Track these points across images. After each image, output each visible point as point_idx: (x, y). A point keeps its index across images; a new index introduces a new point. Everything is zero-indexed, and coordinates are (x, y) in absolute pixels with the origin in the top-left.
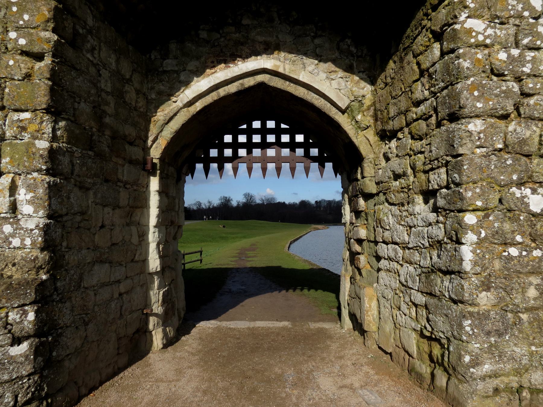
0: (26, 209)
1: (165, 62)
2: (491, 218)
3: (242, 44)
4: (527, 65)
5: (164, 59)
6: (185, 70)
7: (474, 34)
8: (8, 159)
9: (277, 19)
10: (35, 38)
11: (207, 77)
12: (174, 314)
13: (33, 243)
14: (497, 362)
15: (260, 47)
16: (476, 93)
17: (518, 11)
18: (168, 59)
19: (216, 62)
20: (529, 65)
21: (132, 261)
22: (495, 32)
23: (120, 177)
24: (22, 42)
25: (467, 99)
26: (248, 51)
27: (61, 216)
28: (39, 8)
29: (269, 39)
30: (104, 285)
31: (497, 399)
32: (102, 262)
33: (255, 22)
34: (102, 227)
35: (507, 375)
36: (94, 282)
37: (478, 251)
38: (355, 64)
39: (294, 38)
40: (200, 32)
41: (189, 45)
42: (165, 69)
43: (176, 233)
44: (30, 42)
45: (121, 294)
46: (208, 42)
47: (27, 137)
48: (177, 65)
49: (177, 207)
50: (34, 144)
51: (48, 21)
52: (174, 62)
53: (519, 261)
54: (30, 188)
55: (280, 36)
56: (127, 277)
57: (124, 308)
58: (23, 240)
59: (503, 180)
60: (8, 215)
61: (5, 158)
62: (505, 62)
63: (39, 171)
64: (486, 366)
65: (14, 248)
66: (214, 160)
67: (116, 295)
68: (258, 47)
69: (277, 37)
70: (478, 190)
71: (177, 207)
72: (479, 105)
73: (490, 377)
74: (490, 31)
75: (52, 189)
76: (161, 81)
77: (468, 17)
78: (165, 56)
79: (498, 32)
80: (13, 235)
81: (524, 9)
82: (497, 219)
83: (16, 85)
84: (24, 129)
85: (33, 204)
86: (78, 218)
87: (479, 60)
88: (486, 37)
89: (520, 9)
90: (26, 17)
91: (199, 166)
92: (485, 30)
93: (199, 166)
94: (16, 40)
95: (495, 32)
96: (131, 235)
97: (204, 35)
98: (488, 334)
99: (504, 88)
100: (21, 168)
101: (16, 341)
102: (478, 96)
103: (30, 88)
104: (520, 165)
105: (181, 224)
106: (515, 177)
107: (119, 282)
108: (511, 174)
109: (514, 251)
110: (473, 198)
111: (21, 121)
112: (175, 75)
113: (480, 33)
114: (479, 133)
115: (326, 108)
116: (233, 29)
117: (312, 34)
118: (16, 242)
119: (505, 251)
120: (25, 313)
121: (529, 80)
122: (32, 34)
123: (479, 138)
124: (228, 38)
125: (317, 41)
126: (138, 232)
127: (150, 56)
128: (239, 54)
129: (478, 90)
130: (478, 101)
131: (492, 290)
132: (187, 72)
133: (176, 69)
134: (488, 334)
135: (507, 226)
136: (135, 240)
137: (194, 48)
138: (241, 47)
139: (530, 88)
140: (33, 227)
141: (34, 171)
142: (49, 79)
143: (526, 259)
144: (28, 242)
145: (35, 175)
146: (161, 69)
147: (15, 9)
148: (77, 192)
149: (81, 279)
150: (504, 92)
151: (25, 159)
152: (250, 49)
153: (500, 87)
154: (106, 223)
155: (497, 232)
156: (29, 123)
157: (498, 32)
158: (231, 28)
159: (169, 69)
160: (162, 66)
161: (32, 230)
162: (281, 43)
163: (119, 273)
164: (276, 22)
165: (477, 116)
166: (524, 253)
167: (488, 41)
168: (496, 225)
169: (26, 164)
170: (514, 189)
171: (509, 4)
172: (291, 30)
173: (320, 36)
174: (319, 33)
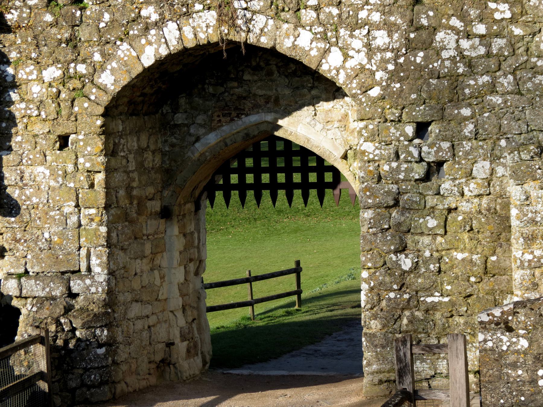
0: (96, 269)
1: (176, 116)
2: (377, 274)
3: (245, 98)
4: (402, 174)
5: (175, 113)
6: (195, 123)
7: (367, 154)
8: (84, 239)
9: (276, 72)
10: (95, 162)
11: (214, 131)
12: (197, 355)
13: (103, 290)
14: (381, 364)
15: (260, 101)
16: (368, 193)
17: (396, 137)
18: (179, 113)
19: (221, 116)
20: (403, 174)
21: (156, 299)
22: (381, 152)
23: (145, 232)
24: (88, 165)
25: (362, 197)
26: (251, 105)
27: (114, 272)
28: (96, 143)
29: (269, 93)
30: (138, 318)
31: (381, 386)
32: (137, 301)
33: (256, 78)
34: (136, 274)
35: (389, 372)
36: (133, 316)
37: (369, 295)
38: (350, 114)
39: (292, 90)
40: (206, 86)
41: (197, 99)
42: (176, 122)
43: (198, 267)
44: (93, 165)
45: (149, 327)
46: (214, 95)
47: (94, 225)
48: (186, 119)
49: (196, 241)
50: (99, 229)
51: (102, 151)
52: (184, 116)
53: (394, 301)
54: (98, 257)
55: (279, 89)
56: (153, 314)
57: (152, 339)
58: (97, 288)
59: (385, 249)
60: (86, 273)
61: (82, 238)
62: (387, 172)
63: (103, 246)
64: (374, 366)
65: (92, 293)
66: (235, 187)
67: (146, 327)
68: (259, 101)
69: (276, 90)
70: (369, 256)
71: (196, 241)
72: (370, 201)
73: (377, 373)
74: (377, 152)
75: (110, 256)
76: (172, 134)
77: (364, 141)
78: (175, 110)
79: (383, 152)
80: (91, 286)
81: (401, 135)
82: (381, 274)
83: (86, 193)
84: (92, 220)
85: (100, 266)
86: (123, 271)
87: (370, 171)
88: (375, 156)
89: (398, 136)
90: (89, 149)
91: (219, 195)
92: (374, 151)
93: (219, 195)
94: (84, 164)
95: (381, 152)
96: (155, 278)
98: (376, 346)
99: (386, 189)
100: (92, 244)
101: (100, 346)
102: (370, 195)
103: (94, 194)
104: (395, 240)
105: (203, 259)
106: (392, 248)
107: (148, 317)
108: (390, 246)
109: (392, 295)
110: (366, 261)
111: (90, 215)
112: (186, 128)
113: (371, 153)
114: (370, 219)
115: (325, 156)
116: (235, 84)
117: (309, 85)
118: (93, 290)
119: (387, 295)
120: (103, 331)
121: (403, 184)
122: (93, 160)
123: (370, 222)
124: (232, 92)
125: (314, 92)
126: (160, 274)
127: (162, 111)
128: (242, 108)
129: (369, 191)
130: (370, 198)
131: (378, 319)
132: (196, 125)
133: (186, 122)
134: (376, 346)
135: (387, 279)
136: (158, 282)
137: (201, 102)
138: (244, 101)
139: (403, 189)
140: (102, 280)
141: (100, 246)
142: (105, 188)
143: (399, 300)
144: (100, 289)
145: (100, 248)
146: (172, 123)
147: (82, 143)
148: (121, 253)
149: (126, 313)
150: (386, 192)
151: (94, 238)
152: (252, 103)
153: (384, 189)
154: (138, 271)
155: (381, 283)
156: (95, 216)
157: (383, 152)
158: (234, 83)
159: (180, 122)
160: (173, 120)
161: (102, 282)
162: (280, 96)
163: (147, 310)
164: (275, 75)
165: (369, 208)
166: (398, 296)
167: (376, 158)
168: (380, 278)
169: (95, 242)
170: (392, 255)
171: (390, 133)
172: (289, 82)
173: (317, 87)
174: (316, 84)
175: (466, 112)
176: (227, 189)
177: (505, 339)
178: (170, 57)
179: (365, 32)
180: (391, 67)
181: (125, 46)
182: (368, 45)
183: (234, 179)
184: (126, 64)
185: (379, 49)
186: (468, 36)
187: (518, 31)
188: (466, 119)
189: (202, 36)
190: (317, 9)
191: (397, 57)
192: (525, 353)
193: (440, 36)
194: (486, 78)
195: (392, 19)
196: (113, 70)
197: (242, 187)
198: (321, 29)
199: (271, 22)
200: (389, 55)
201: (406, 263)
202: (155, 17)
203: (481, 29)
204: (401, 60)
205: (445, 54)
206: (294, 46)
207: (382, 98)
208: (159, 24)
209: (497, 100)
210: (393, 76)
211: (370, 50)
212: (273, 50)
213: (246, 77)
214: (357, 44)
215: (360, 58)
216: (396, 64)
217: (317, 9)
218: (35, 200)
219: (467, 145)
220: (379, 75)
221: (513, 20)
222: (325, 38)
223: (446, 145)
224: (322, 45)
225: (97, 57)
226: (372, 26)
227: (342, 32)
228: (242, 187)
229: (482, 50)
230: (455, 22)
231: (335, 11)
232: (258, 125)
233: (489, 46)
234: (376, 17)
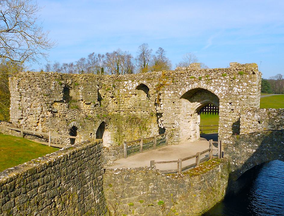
97: (199, 95)
175: (238, 101)
176: (203, 111)
177: (228, 142)
178: (190, 90)
179: (222, 87)
180: (225, 93)
181: (183, 88)
182: (222, 89)
183: (204, 110)
184: (183, 91)
185: (224, 90)
186: (239, 88)
187: (248, 88)
188: (237, 102)
189: (195, 87)
190: (214, 83)
191: (226, 92)
192: (232, 144)
193: (234, 88)
194: (242, 96)
195: (226, 85)
196: (181, 92)
197: (206, 111)
198: (214, 86)
199: (206, 85)
200: (225, 91)
201: (226, 126)
202: (188, 84)
203: (241, 87)
204: (227, 92)
205: (235, 91)
206: (210, 89)
207: (223, 98)
208: (189, 85)
209: (243, 99)
210: (226, 95)
211: (222, 90)
212: (207, 90)
213: (205, 94)
214: (220, 89)
215: (220, 92)
216: (226, 93)
217: (214, 83)
218: (169, 112)
219: (238, 107)
220: (224, 94)
221: (247, 86)
222: (215, 88)
223: (234, 107)
224: (214, 89)
225: (179, 90)
226: (223, 86)
227: (218, 87)
228: (206, 111)
229: (241, 91)
230: (237, 86)
231: (217, 83)
232: (206, 102)
233: (242, 91)
234: (224, 85)
